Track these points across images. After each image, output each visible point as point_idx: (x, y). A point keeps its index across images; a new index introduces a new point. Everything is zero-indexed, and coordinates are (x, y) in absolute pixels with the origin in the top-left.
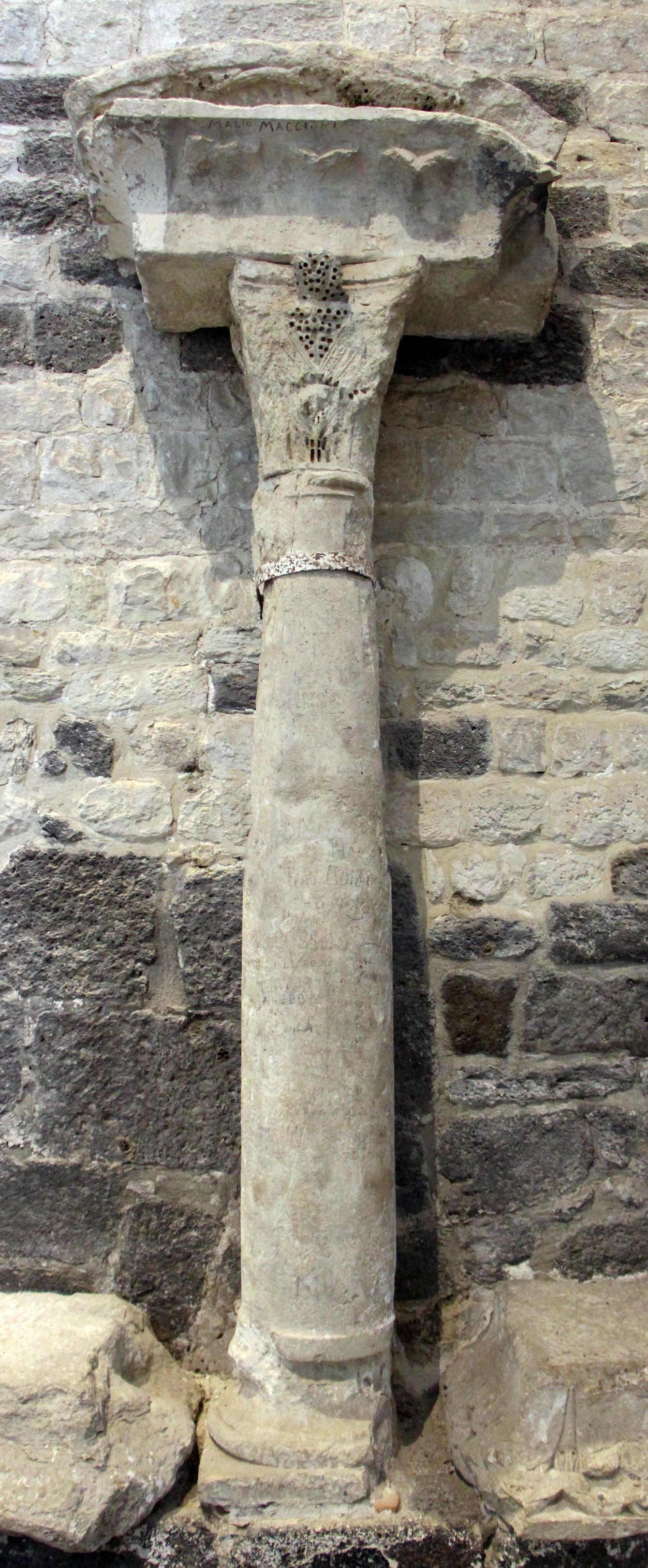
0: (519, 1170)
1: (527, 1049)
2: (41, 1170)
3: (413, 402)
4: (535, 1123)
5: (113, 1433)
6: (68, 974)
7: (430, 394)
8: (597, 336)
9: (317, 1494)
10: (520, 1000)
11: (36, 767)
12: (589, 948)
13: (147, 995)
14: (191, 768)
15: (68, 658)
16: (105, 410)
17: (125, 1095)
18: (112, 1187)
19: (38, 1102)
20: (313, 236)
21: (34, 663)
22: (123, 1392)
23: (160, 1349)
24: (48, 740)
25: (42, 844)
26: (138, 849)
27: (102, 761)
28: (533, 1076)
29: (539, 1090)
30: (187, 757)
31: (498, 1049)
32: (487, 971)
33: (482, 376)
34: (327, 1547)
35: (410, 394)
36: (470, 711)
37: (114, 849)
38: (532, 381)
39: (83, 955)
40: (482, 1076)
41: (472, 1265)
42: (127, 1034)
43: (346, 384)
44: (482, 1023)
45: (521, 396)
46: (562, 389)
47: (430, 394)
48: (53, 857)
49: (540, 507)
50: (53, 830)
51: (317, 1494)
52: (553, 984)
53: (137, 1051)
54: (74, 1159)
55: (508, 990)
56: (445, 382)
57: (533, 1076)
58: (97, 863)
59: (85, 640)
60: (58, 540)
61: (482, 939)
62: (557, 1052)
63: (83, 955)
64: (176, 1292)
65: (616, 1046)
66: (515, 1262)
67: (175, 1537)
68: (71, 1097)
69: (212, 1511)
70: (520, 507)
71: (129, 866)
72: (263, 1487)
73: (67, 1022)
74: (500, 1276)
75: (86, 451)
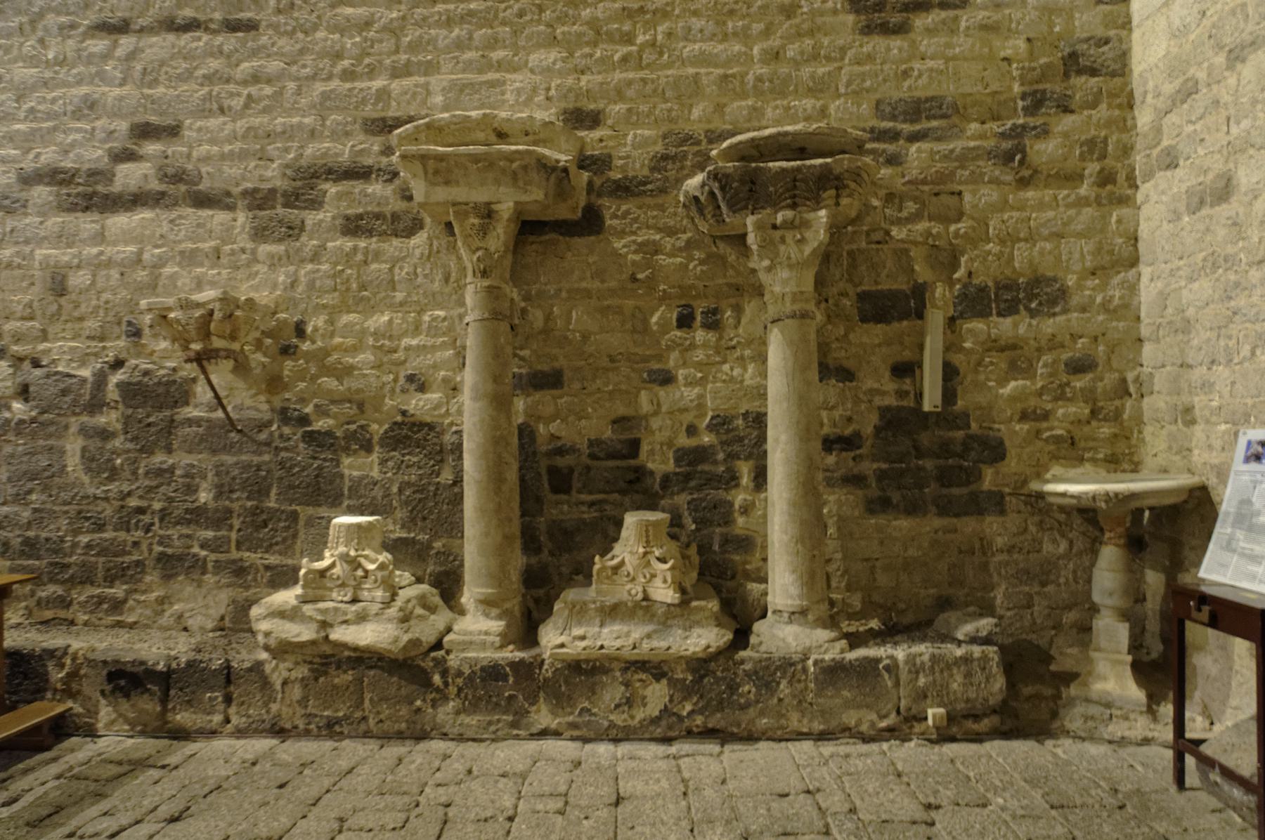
0: (578, 539)
1: (579, 492)
2: (400, 539)
3: (534, 246)
4: (584, 522)
5: (412, 622)
6: (408, 467)
7: (541, 242)
8: (607, 214)
9: (483, 646)
10: (576, 475)
11: (398, 390)
12: (602, 455)
13: (438, 475)
14: (454, 389)
15: (408, 349)
16: (418, 252)
17: (431, 512)
18: (429, 546)
19: (399, 514)
20: (480, 195)
21: (395, 352)
22: (419, 611)
23: (441, 603)
24: (402, 381)
25: (399, 418)
26: (435, 420)
27: (422, 388)
28: (583, 503)
29: (584, 508)
30: (452, 385)
31: (567, 491)
32: (561, 462)
33: (561, 234)
34: (485, 663)
35: (533, 243)
36: (556, 365)
37: (428, 419)
38: (581, 235)
39: (415, 459)
40: (562, 503)
41: (560, 574)
42: (432, 488)
43: (492, 249)
44: (561, 482)
45: (577, 241)
46: (593, 238)
47: (541, 242)
48: (403, 423)
49: (584, 285)
50: (404, 413)
51: (483, 646)
52: (588, 468)
53: (435, 495)
54: (412, 535)
55: (571, 470)
56: (547, 237)
57: (583, 503)
58: (422, 425)
59: (414, 342)
60: (401, 304)
61: (560, 451)
62: (590, 493)
63: (415, 459)
64: (448, 586)
65: (612, 492)
66: (577, 574)
67: (434, 659)
68: (411, 511)
69: (448, 652)
70: (576, 286)
71: (431, 427)
72: (464, 643)
73: (409, 484)
74: (571, 579)
75: (411, 270)
